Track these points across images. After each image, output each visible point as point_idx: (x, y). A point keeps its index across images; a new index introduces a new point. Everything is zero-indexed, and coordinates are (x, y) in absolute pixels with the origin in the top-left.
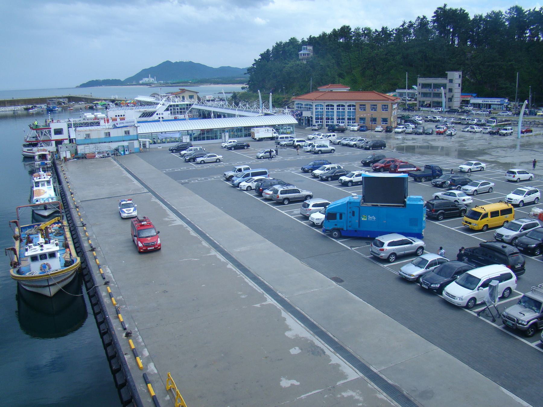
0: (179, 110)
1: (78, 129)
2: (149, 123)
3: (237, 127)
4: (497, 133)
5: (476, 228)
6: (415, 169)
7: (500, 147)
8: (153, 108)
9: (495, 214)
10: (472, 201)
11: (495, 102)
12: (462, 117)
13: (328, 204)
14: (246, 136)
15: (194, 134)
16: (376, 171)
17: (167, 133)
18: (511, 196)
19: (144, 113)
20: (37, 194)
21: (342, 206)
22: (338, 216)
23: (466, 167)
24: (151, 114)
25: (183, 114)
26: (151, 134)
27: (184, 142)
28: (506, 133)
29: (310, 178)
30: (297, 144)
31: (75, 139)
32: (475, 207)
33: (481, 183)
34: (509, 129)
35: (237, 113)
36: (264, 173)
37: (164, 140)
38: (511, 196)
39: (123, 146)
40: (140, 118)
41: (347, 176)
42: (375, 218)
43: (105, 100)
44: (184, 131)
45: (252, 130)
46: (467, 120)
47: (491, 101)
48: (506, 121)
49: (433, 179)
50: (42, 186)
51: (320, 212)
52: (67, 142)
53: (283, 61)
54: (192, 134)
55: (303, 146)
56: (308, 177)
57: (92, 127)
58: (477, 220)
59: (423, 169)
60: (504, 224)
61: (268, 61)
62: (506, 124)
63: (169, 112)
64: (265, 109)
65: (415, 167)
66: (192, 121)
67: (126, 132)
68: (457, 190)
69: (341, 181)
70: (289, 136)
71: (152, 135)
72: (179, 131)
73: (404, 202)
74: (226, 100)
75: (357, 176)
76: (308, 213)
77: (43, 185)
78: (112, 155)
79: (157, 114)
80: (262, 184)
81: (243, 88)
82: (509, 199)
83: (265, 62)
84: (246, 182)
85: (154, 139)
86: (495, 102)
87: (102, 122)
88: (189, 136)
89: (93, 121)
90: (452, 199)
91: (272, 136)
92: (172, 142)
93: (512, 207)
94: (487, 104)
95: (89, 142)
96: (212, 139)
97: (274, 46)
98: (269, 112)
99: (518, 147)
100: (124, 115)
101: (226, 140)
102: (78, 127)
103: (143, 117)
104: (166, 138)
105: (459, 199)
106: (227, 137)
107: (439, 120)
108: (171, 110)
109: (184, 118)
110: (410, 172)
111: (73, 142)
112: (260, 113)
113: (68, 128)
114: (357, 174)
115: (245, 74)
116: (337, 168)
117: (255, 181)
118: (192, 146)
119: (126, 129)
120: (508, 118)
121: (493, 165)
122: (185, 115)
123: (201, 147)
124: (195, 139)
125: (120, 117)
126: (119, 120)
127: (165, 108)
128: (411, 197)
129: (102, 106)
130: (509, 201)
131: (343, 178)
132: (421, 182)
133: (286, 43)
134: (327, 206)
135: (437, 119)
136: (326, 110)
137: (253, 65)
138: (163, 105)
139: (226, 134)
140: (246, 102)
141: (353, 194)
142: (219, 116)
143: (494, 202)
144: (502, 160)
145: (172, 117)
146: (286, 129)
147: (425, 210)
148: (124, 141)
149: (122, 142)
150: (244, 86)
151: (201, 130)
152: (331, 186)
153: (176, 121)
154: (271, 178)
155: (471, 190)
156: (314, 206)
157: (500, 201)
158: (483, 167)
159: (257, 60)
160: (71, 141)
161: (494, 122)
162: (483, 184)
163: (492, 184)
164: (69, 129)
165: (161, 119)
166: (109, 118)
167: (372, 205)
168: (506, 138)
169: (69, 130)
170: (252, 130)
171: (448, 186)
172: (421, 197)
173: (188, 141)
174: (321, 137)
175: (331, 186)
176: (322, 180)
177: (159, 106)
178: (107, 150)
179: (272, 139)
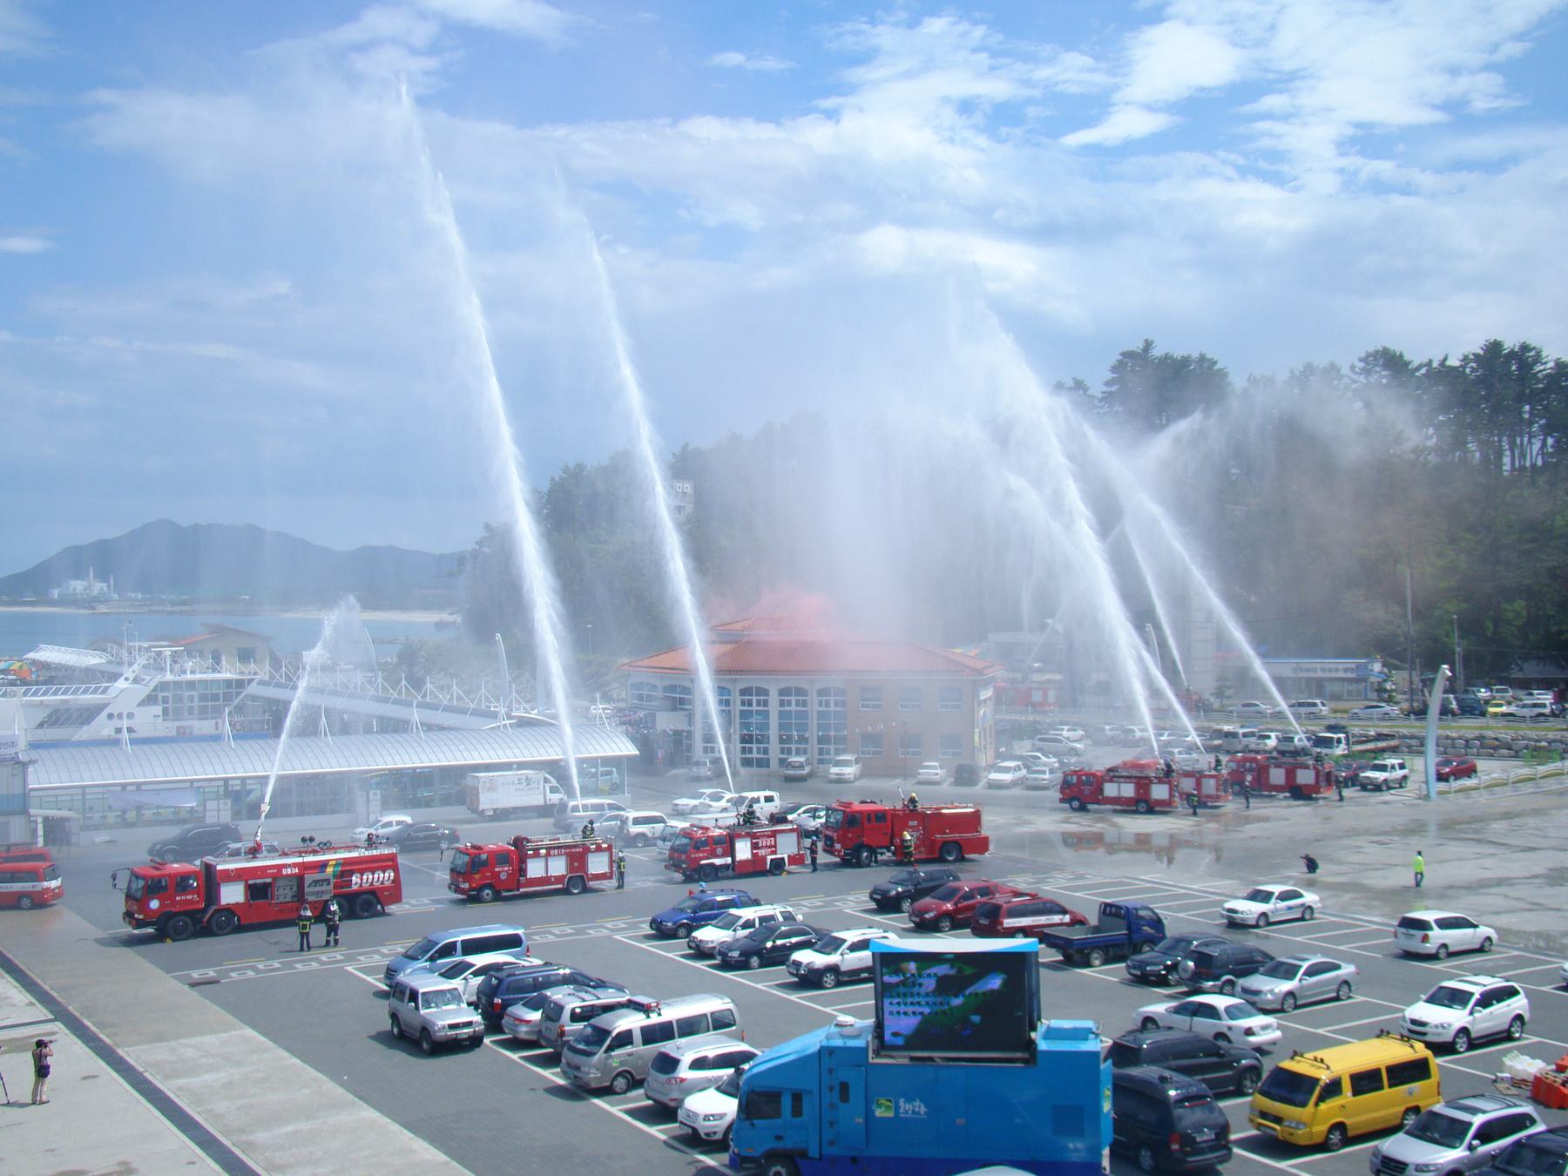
0: (196, 703)
3: (414, 769)
4: (1353, 780)
5: (1301, 1136)
6: (1067, 918)
7: (1366, 832)
8: (95, 692)
9: (1366, 1081)
10: (1278, 1034)
11: (1337, 670)
12: (1226, 728)
13: (747, 1057)
14: (446, 801)
15: (249, 792)
16: (925, 926)
17: (143, 787)
18: (1423, 1011)
19: (57, 711)
21: (802, 1062)
22: (786, 1103)
23: (1249, 909)
24: (88, 715)
26: (79, 791)
27: (209, 821)
28: (1385, 780)
29: (684, 956)
30: (635, 829)
32: (1292, 1058)
33: (1308, 968)
34: (1393, 767)
35: (416, 715)
36: (511, 942)
37: (131, 815)
38: (1423, 1011)
40: (40, 731)
41: (816, 947)
42: (923, 1109)
44: (213, 783)
46: (1245, 735)
47: (1323, 670)
48: (1380, 737)
49: (1133, 954)
51: (718, 1089)
55: (655, 838)
56: (673, 952)
58: (1303, 1104)
59: (1093, 920)
60: (1404, 1118)
62: (1383, 750)
63: (158, 710)
64: (519, 703)
65: (1064, 911)
66: (240, 742)
68: (1221, 993)
69: (798, 970)
71: (84, 794)
72: (192, 781)
73: (1032, 1043)
75: (855, 947)
76: (675, 1095)
79: (110, 716)
80: (500, 981)
81: (440, 626)
82: (1414, 1022)
84: (442, 975)
85: (91, 808)
86: (1337, 670)
88: (229, 801)
90: (1204, 1026)
91: (542, 803)
92: (162, 823)
93: (1428, 1053)
94: (1308, 680)
96: (320, 811)
97: (557, 479)
98: (534, 714)
99: (1432, 828)
101: (372, 818)
104: (139, 808)
105: (1230, 1028)
106: (376, 804)
107: (1142, 739)
108: (165, 700)
109: (213, 731)
110: (1046, 930)
112: (500, 716)
114: (856, 940)
116: (781, 919)
117: (476, 974)
118: (239, 840)
120: (1388, 727)
121: (1346, 897)
122: (220, 721)
123: (276, 843)
127: (143, 691)
128: (1055, 1023)
130: (1416, 1030)
131: (805, 957)
132: (1088, 965)
134: (746, 1066)
135: (1138, 734)
136: (739, 707)
138: (136, 681)
139: (371, 792)
141: (843, 1018)
143: (1361, 1034)
144: (1378, 880)
146: (595, 775)
147: (1106, 1066)
150: (446, 617)
152: (759, 986)
153: (183, 745)
154: (537, 962)
155: (1271, 991)
156: (698, 1064)
157: (1382, 1031)
158: (1310, 907)
161: (1339, 741)
162: (1311, 972)
163: (1347, 970)
165: (125, 735)
167: (912, 1059)
168: (1387, 796)
170: (469, 782)
171: (1189, 980)
172: (1089, 1024)
173: (226, 817)
174: (723, 803)
175: (759, 986)
176: (727, 965)
177: (121, 684)
179: (545, 810)
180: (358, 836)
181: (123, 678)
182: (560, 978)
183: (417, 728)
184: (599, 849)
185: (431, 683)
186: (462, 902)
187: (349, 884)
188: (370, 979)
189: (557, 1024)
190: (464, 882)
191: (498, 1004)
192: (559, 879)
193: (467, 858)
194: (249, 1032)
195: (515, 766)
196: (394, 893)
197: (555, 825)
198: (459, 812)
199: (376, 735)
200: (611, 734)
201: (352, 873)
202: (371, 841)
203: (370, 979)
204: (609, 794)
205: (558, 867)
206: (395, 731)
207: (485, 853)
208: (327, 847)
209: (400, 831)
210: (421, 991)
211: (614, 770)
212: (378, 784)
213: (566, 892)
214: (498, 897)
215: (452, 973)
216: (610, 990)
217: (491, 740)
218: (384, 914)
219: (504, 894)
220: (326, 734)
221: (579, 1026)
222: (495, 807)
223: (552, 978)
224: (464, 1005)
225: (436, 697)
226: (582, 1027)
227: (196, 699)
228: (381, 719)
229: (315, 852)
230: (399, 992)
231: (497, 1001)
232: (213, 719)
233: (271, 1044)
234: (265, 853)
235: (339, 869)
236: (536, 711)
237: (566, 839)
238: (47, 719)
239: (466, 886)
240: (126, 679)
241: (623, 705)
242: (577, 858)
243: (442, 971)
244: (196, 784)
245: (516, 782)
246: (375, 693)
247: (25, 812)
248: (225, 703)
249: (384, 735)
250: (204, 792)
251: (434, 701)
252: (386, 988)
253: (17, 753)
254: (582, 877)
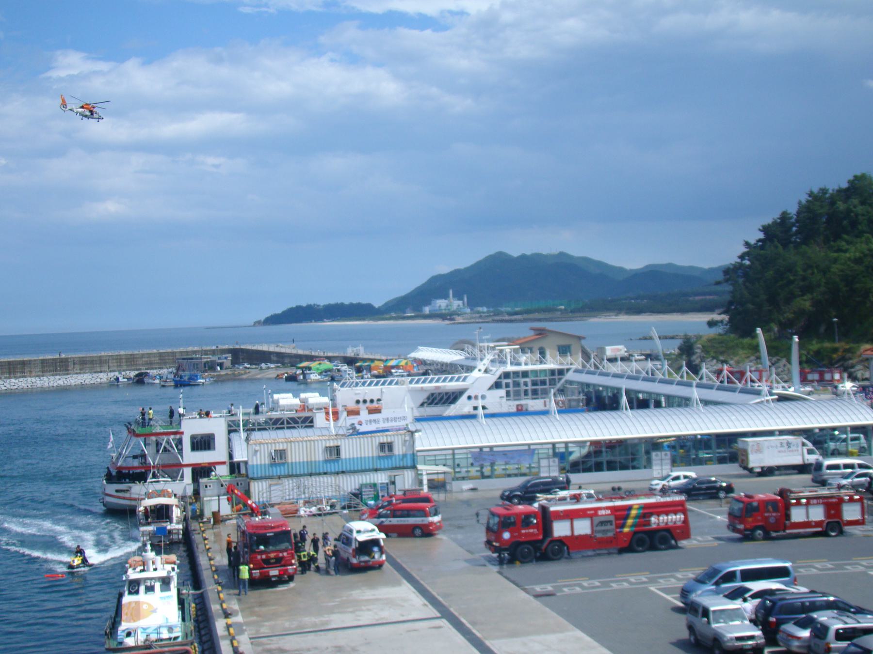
0: (530, 387)
1: (257, 436)
2: (446, 423)
3: (695, 435)
8: (458, 380)
14: (722, 460)
15: (571, 453)
19: (432, 394)
24: (452, 397)
25: (540, 396)
26: (451, 452)
27: (542, 475)
31: (246, 463)
35: (695, 393)
36: (780, 573)
39: (374, 485)
40: (422, 409)
43: (330, 359)
45: (740, 443)
50: (146, 593)
52: (223, 471)
53: (832, 243)
54: (566, 454)
57: (293, 431)
61: (785, 246)
63: (502, 392)
64: (778, 382)
66: (564, 416)
67: (382, 446)
70: (855, 461)
71: (454, 454)
72: (529, 445)
74: (662, 357)
77: (150, 589)
78: (344, 508)
79: (469, 398)
80: (774, 603)
81: (711, 324)
83: (776, 247)
84: (727, 596)
85: (458, 465)
87: (320, 419)
88: (556, 460)
89: (293, 414)
92: (509, 476)
95: (282, 471)
96: (624, 467)
97: (804, 202)
98: (791, 391)
100: (379, 400)
102: (254, 430)
103: (430, 404)
111: (239, 471)
112: (763, 393)
113: (230, 432)
115: (718, 283)
117: (754, 596)
119: (384, 439)
123: (592, 492)
124: (577, 467)
125: (368, 404)
126: (364, 415)
127: (492, 379)
129: (320, 374)
133: (840, 191)
137: (742, 257)
138: (486, 371)
140: (723, 362)
142: (640, 403)
145: (510, 406)
146: (845, 440)
148: (376, 470)
149: (371, 474)
150: (716, 317)
151: (594, 443)
153: (522, 418)
154: (803, 589)
159: (752, 241)
160: (234, 468)
164: (232, 434)
165: (480, 411)
166: (340, 408)
169: (229, 440)
173: (555, 473)
177: (475, 374)
178: (330, 494)
179: (802, 469)
180: (654, 487)
181: (476, 371)
182: (824, 603)
183: (697, 404)
184: (851, 500)
185: (707, 368)
186: (740, 540)
187: (649, 523)
188: (669, 597)
189: (822, 641)
190: (740, 523)
191: (772, 622)
192: (818, 524)
193: (741, 505)
194: (579, 633)
195: (777, 433)
196: (684, 531)
197: (814, 481)
198: (733, 469)
199: (665, 409)
200: (858, 407)
201: (651, 514)
202: (664, 491)
203: (669, 597)
204: (859, 455)
205: (817, 514)
206: (679, 406)
207: (754, 501)
208: (631, 494)
209: (687, 484)
210: (712, 609)
211: (862, 436)
212: (669, 446)
213: (824, 534)
214: (767, 537)
215: (735, 595)
216: (869, 616)
217: (756, 412)
218: (676, 547)
219: (774, 534)
220: (626, 409)
221: (843, 644)
222: (762, 465)
223: (818, 604)
224: (747, 622)
225: (710, 379)
226: (846, 645)
227: (530, 384)
228: (669, 398)
229: (622, 498)
230: (692, 609)
231: (772, 619)
232: (542, 398)
233: (595, 644)
234: (585, 498)
235: (641, 511)
236: (792, 389)
237: (824, 492)
238: (426, 401)
239: (741, 527)
240: (479, 370)
241: (866, 383)
242: (833, 507)
243: (726, 593)
244: (532, 447)
245: (779, 445)
246: (663, 377)
247: (414, 467)
248: (551, 386)
249: (671, 409)
250: (538, 453)
251: (710, 382)
252: (681, 605)
253: (407, 425)
254: (838, 522)
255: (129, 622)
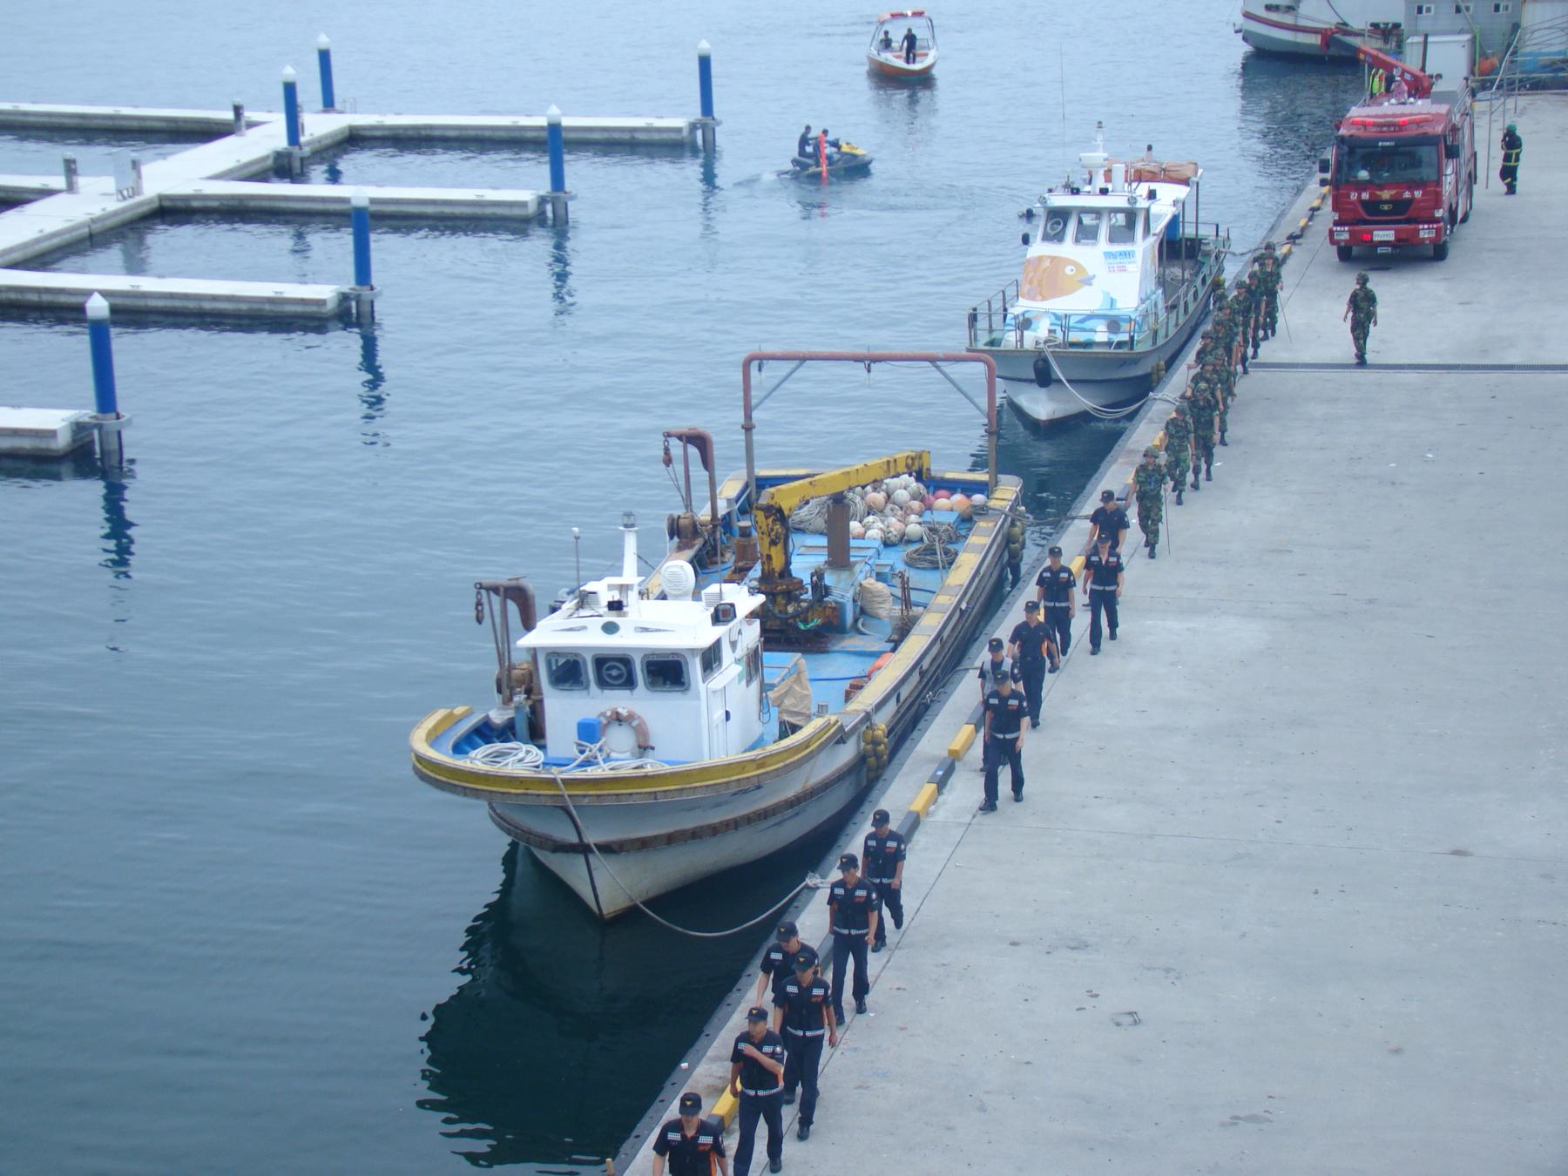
20: (1040, 285)
50: (1077, 241)
77: (1087, 234)
255: (1033, 299)
